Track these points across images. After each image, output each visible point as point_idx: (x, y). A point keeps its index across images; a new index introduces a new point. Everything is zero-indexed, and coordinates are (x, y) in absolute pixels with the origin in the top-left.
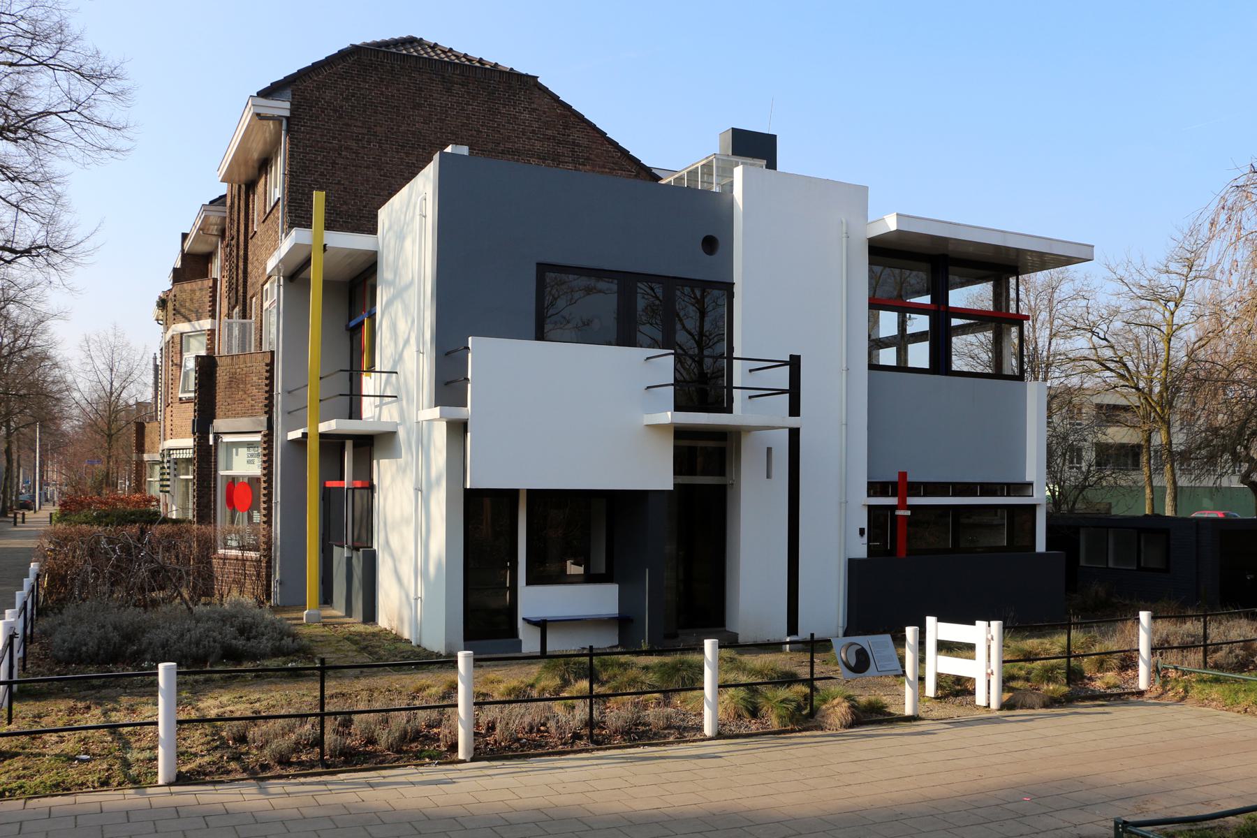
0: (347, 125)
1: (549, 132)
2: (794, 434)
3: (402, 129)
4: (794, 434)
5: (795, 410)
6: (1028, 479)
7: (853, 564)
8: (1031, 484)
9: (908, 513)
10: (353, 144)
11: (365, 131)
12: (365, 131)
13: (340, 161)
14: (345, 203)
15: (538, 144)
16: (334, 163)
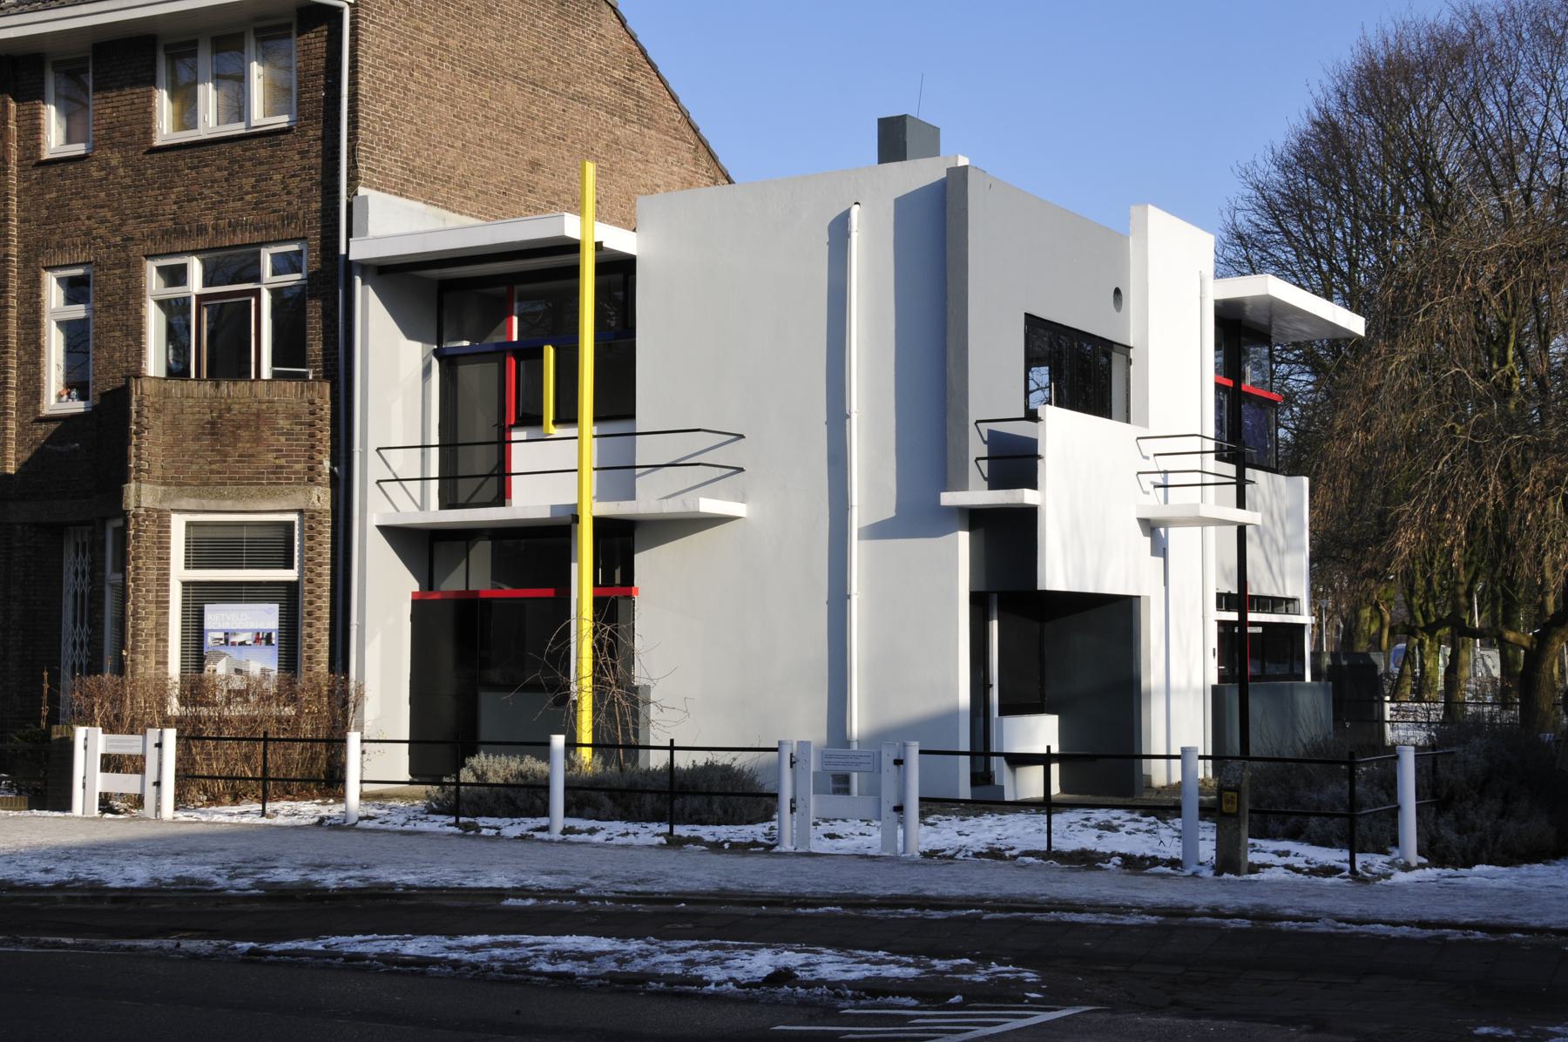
0: (417, 28)
1: (616, 74)
2: (1242, 530)
3: (476, 44)
4: (1242, 530)
5: (1241, 503)
6: (1289, 595)
7: (1214, 687)
8: (1293, 600)
9: (1259, 630)
10: (423, 59)
11: (437, 42)
12: (437, 42)
13: (412, 86)
14: (418, 154)
15: (606, 90)
16: (406, 88)
